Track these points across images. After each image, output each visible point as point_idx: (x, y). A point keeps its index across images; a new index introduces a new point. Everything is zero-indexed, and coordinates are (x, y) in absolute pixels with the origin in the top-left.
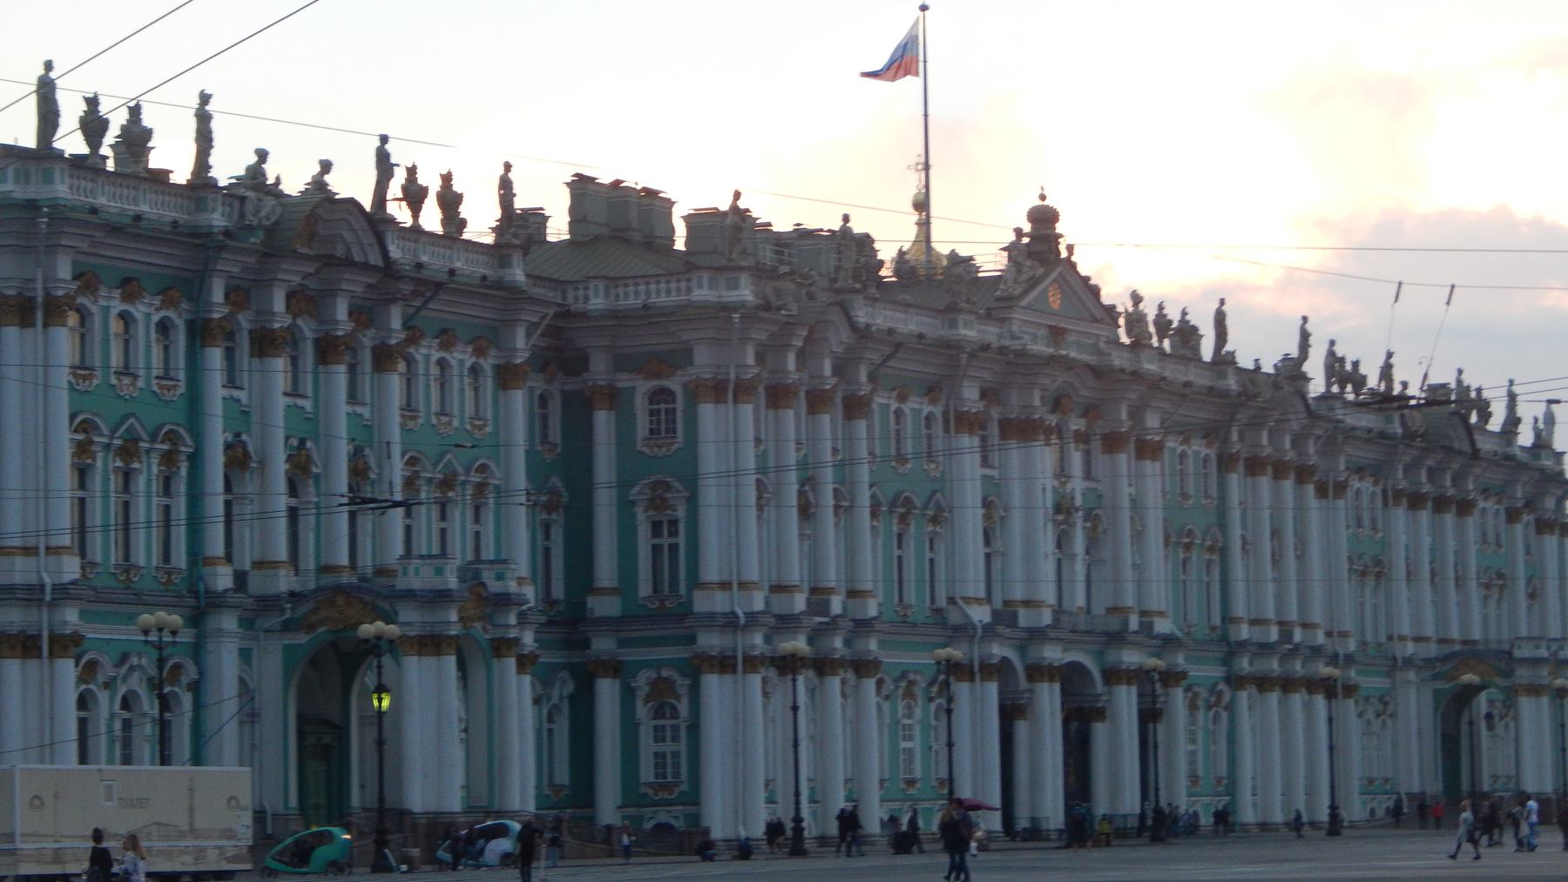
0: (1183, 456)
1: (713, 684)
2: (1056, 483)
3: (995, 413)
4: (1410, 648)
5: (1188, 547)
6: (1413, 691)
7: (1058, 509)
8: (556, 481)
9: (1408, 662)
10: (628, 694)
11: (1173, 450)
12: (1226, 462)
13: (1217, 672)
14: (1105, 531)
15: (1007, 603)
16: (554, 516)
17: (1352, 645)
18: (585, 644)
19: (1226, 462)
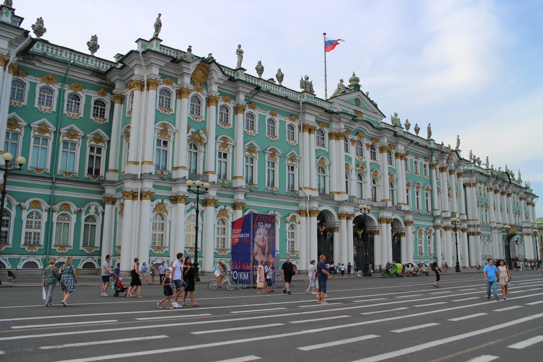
0: (415, 162)
1: (128, 203)
2: (358, 158)
4: (495, 225)
5: (418, 187)
6: (497, 235)
7: (358, 166)
9: (495, 228)
10: (116, 209)
11: (411, 160)
12: (432, 166)
13: (431, 224)
14: (380, 176)
15: (331, 193)
16: (101, 144)
17: (479, 223)
18: (104, 192)
19: (432, 166)
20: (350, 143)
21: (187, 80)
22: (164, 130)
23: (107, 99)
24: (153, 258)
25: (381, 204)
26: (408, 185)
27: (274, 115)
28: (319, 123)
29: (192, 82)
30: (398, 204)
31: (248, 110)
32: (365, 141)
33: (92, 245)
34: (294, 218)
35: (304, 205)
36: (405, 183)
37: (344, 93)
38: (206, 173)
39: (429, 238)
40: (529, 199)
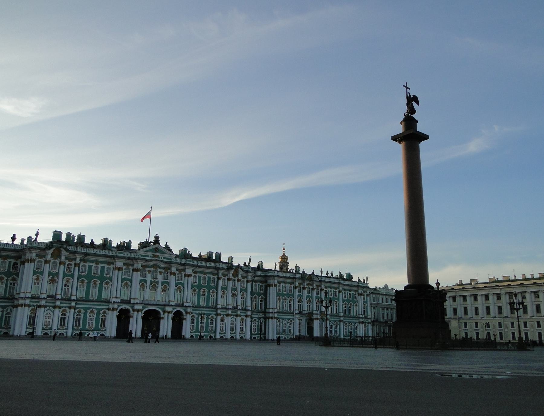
0: (205, 277)
3: (131, 268)
5: (204, 292)
7: (151, 284)
8: (15, 276)
9: (296, 314)
12: (219, 279)
17: (276, 310)
19: (219, 279)
21: (49, 257)
22: (37, 279)
23: (18, 262)
24: (28, 330)
25: (167, 303)
26: (195, 291)
28: (124, 264)
29: (52, 255)
30: (183, 302)
31: (82, 264)
33: (8, 324)
34: (105, 312)
35: (111, 306)
36: (190, 290)
37: (146, 247)
38: (56, 294)
39: (212, 320)
40: (360, 291)
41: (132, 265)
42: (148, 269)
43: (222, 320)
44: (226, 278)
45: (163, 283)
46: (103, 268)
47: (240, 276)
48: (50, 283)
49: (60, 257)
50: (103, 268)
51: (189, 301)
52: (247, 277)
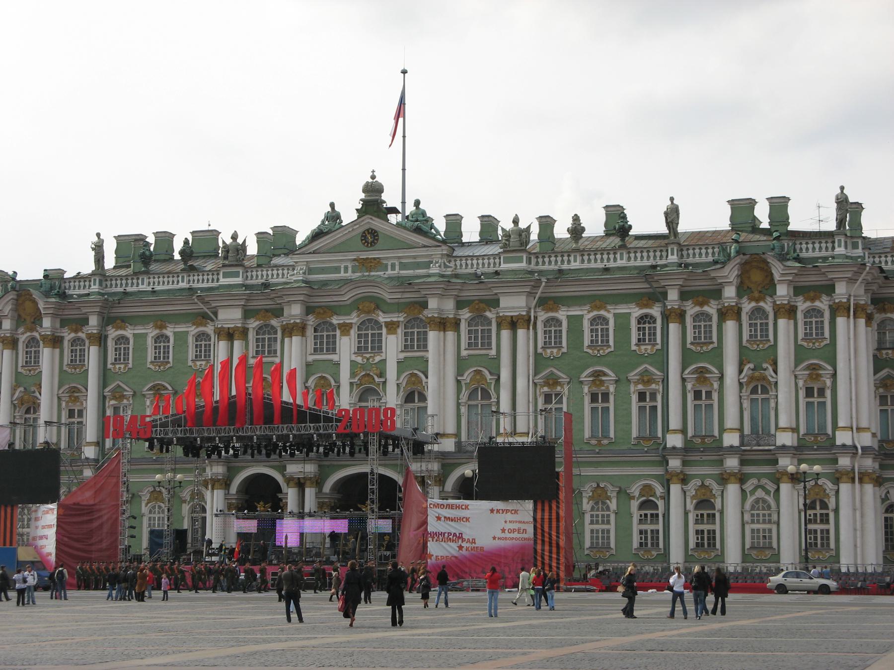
2: (359, 359)
3: (274, 322)
7: (353, 374)
19: (667, 317)
20: (338, 332)
27: (165, 327)
31: (113, 333)
32: (382, 318)
41: (278, 312)
42: (335, 320)
43: (704, 503)
44: (711, 309)
45: (402, 365)
46: (181, 338)
47: (782, 291)
48: (28, 411)
49: (37, 318)
50: (181, 338)
51: (521, 427)
52: (830, 289)
